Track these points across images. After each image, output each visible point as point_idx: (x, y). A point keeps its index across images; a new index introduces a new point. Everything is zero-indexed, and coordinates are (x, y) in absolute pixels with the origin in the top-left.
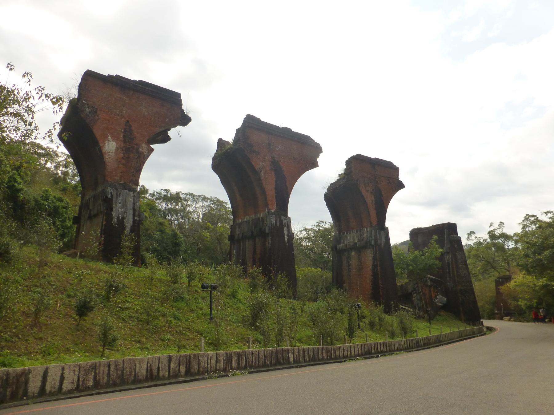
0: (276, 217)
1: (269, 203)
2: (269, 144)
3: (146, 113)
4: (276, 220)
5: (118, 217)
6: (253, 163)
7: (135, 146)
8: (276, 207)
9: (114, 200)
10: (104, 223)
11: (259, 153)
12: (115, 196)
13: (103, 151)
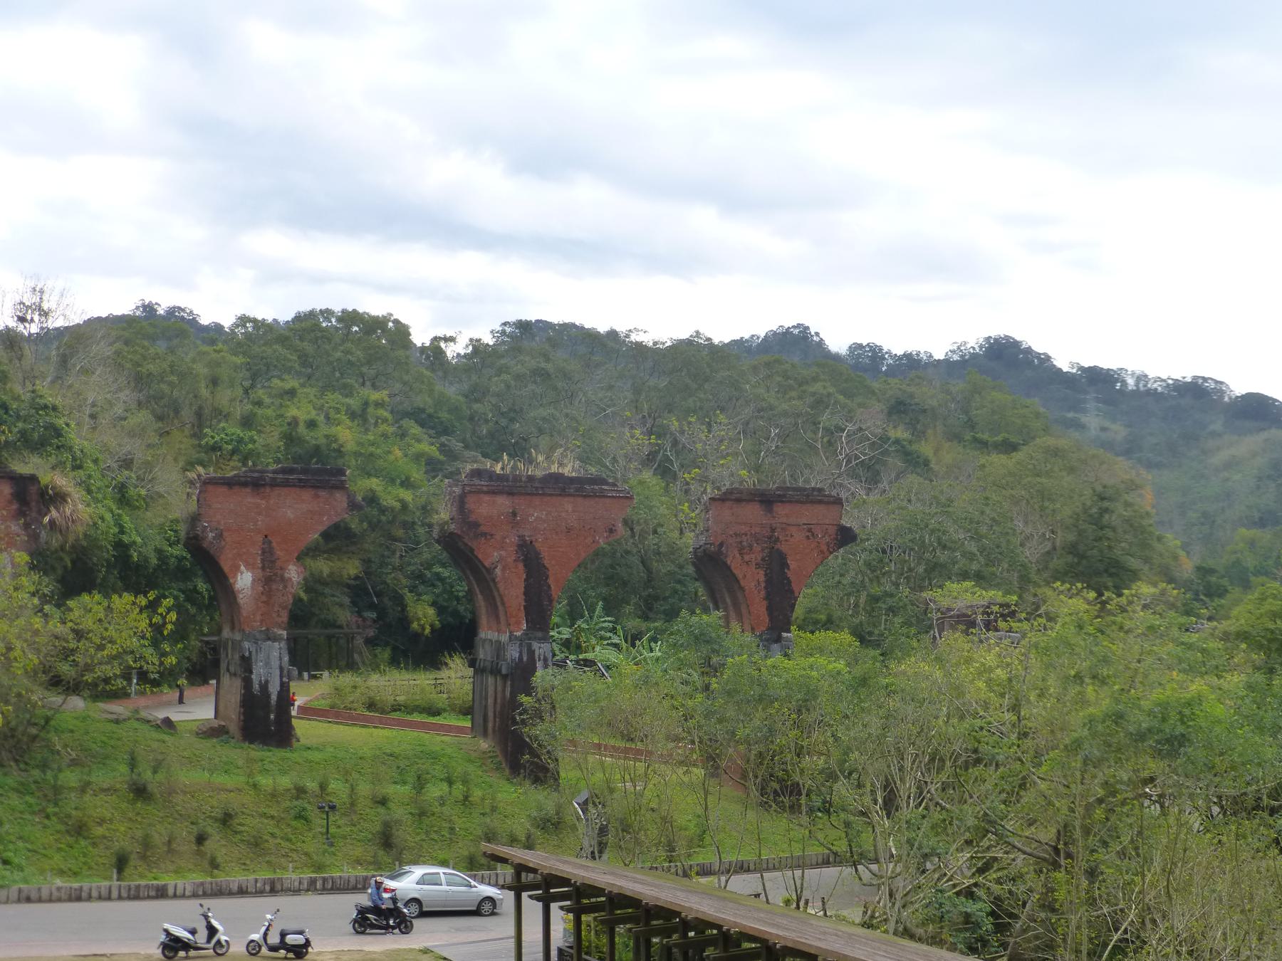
0: (521, 645)
1: (513, 620)
2: (514, 514)
5: (260, 681)
6: (480, 556)
7: (279, 572)
8: (524, 627)
10: (243, 692)
11: (492, 535)
12: (254, 653)
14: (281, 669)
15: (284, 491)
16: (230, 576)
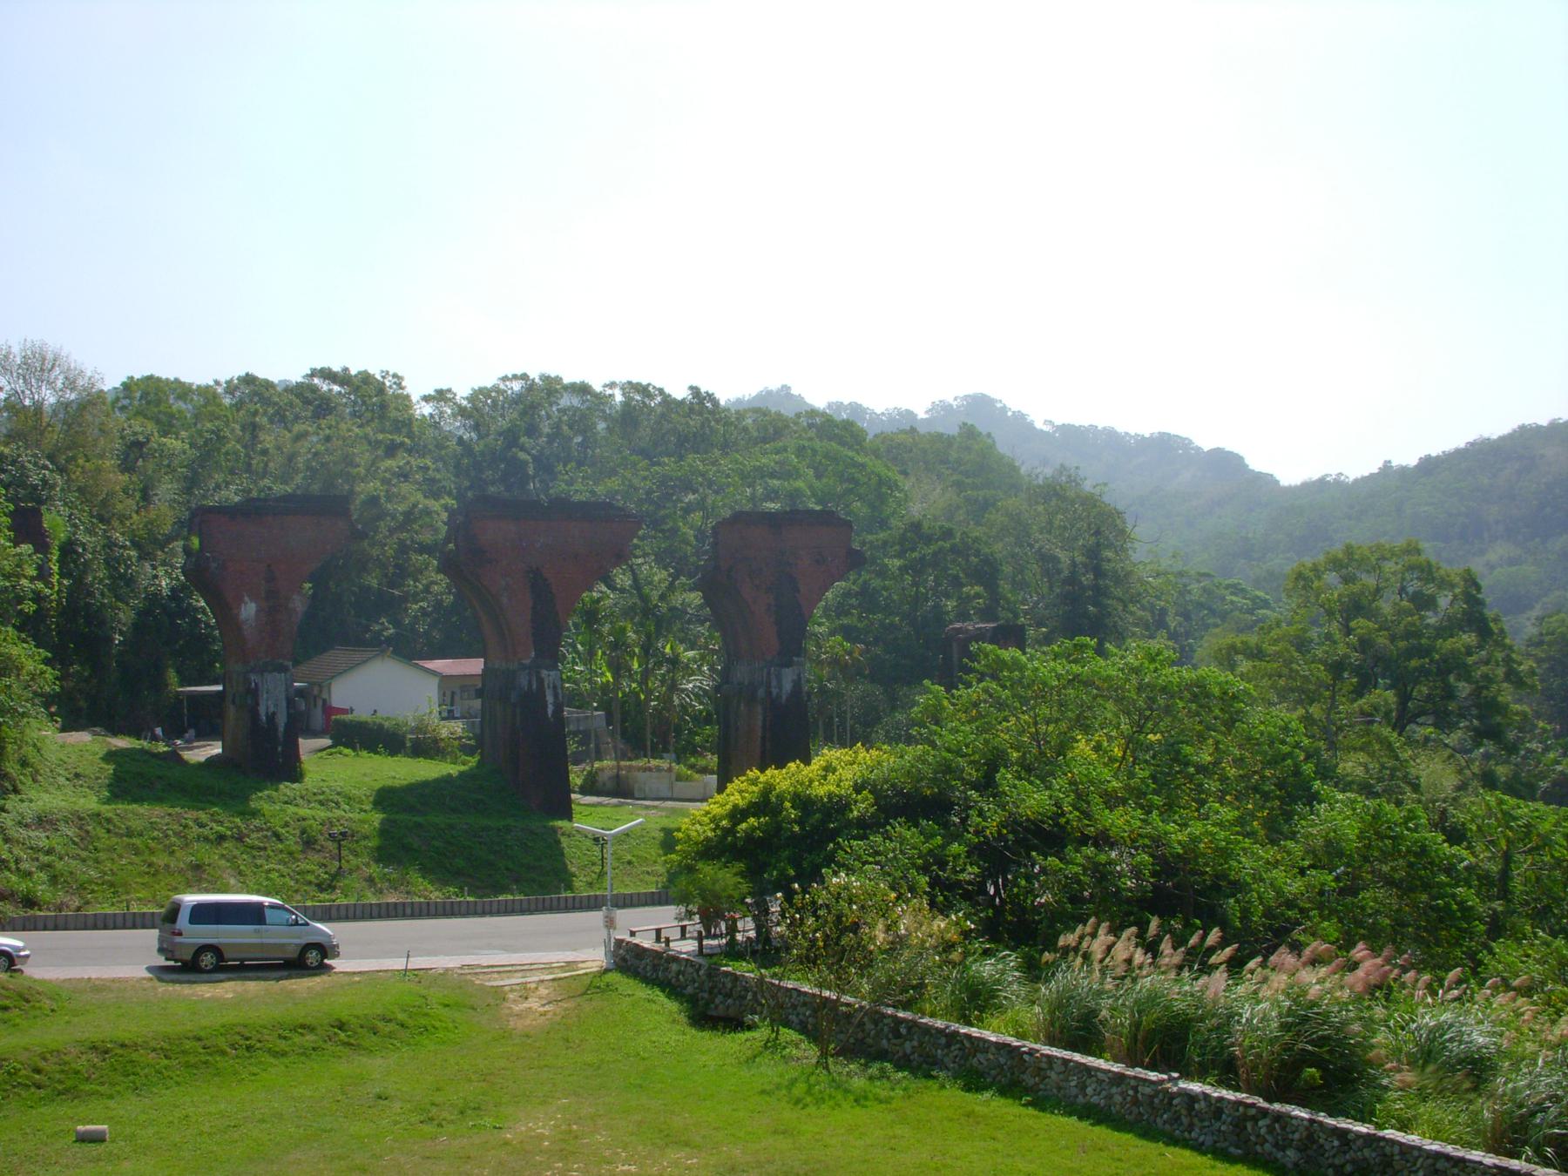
12: (260, 684)
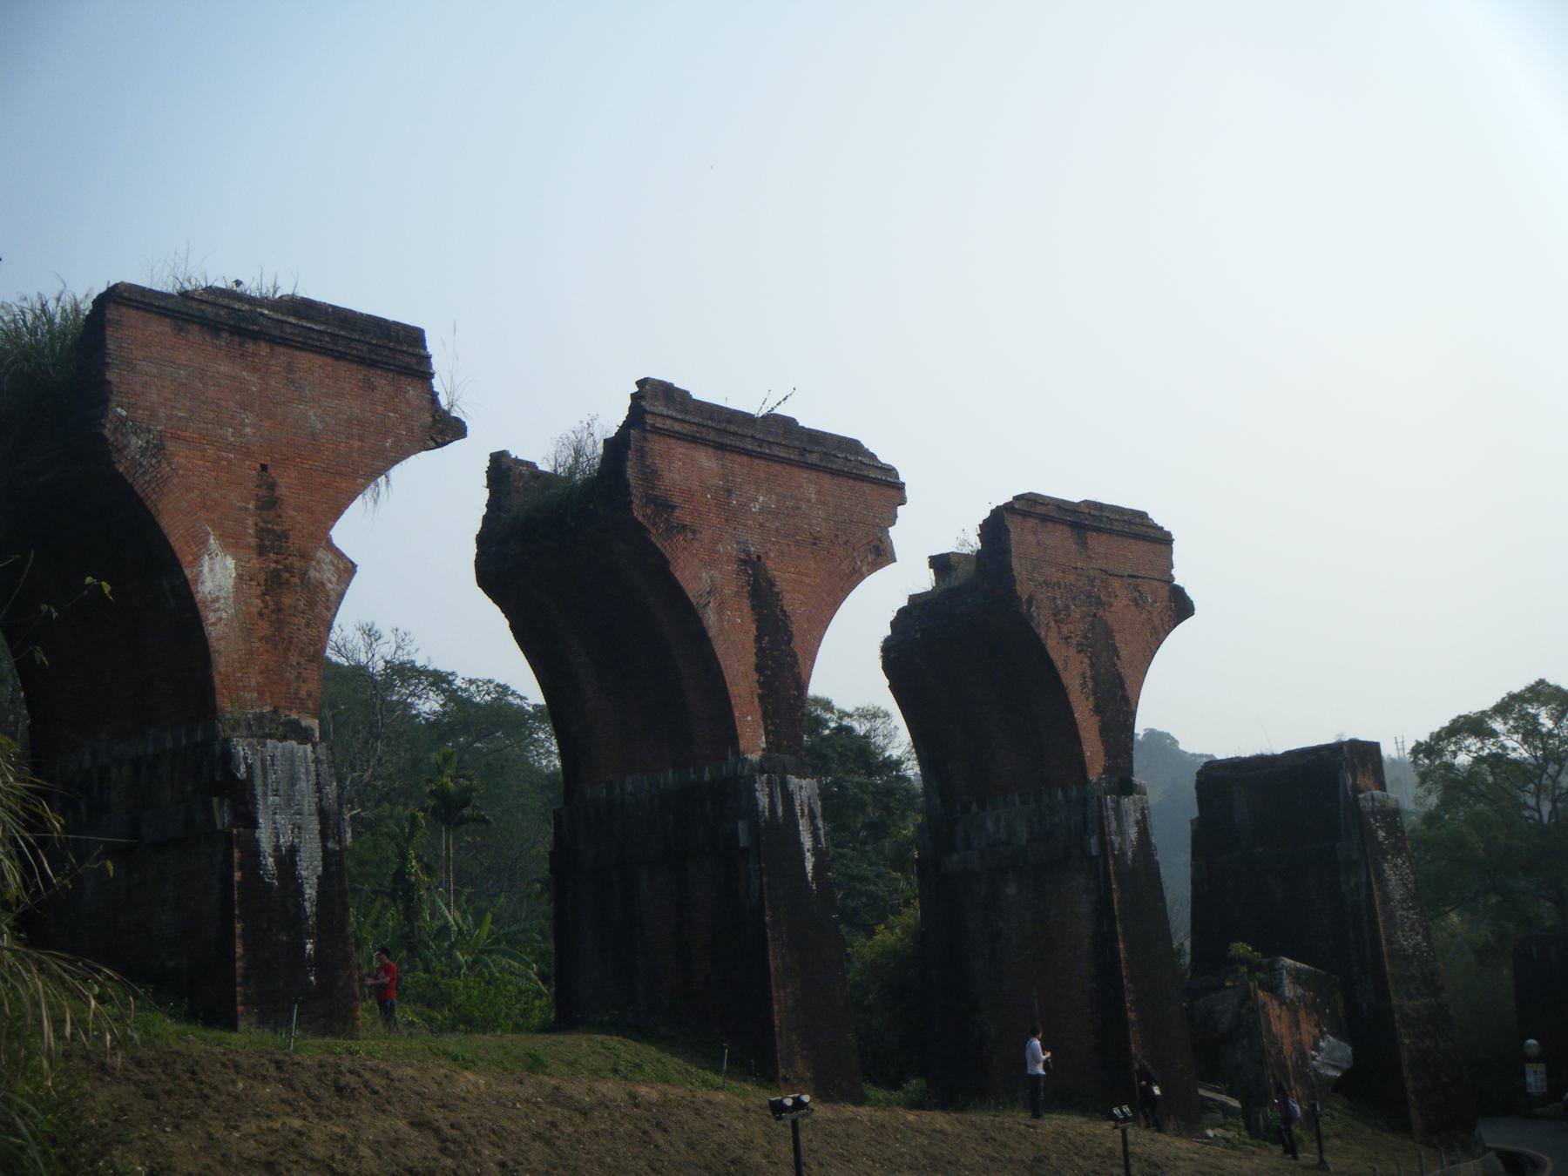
3: (319, 426)
4: (771, 796)
7: (298, 564)
9: (258, 781)
13: (198, 597)
14: (323, 814)
15: (303, 358)
16: (185, 559)
